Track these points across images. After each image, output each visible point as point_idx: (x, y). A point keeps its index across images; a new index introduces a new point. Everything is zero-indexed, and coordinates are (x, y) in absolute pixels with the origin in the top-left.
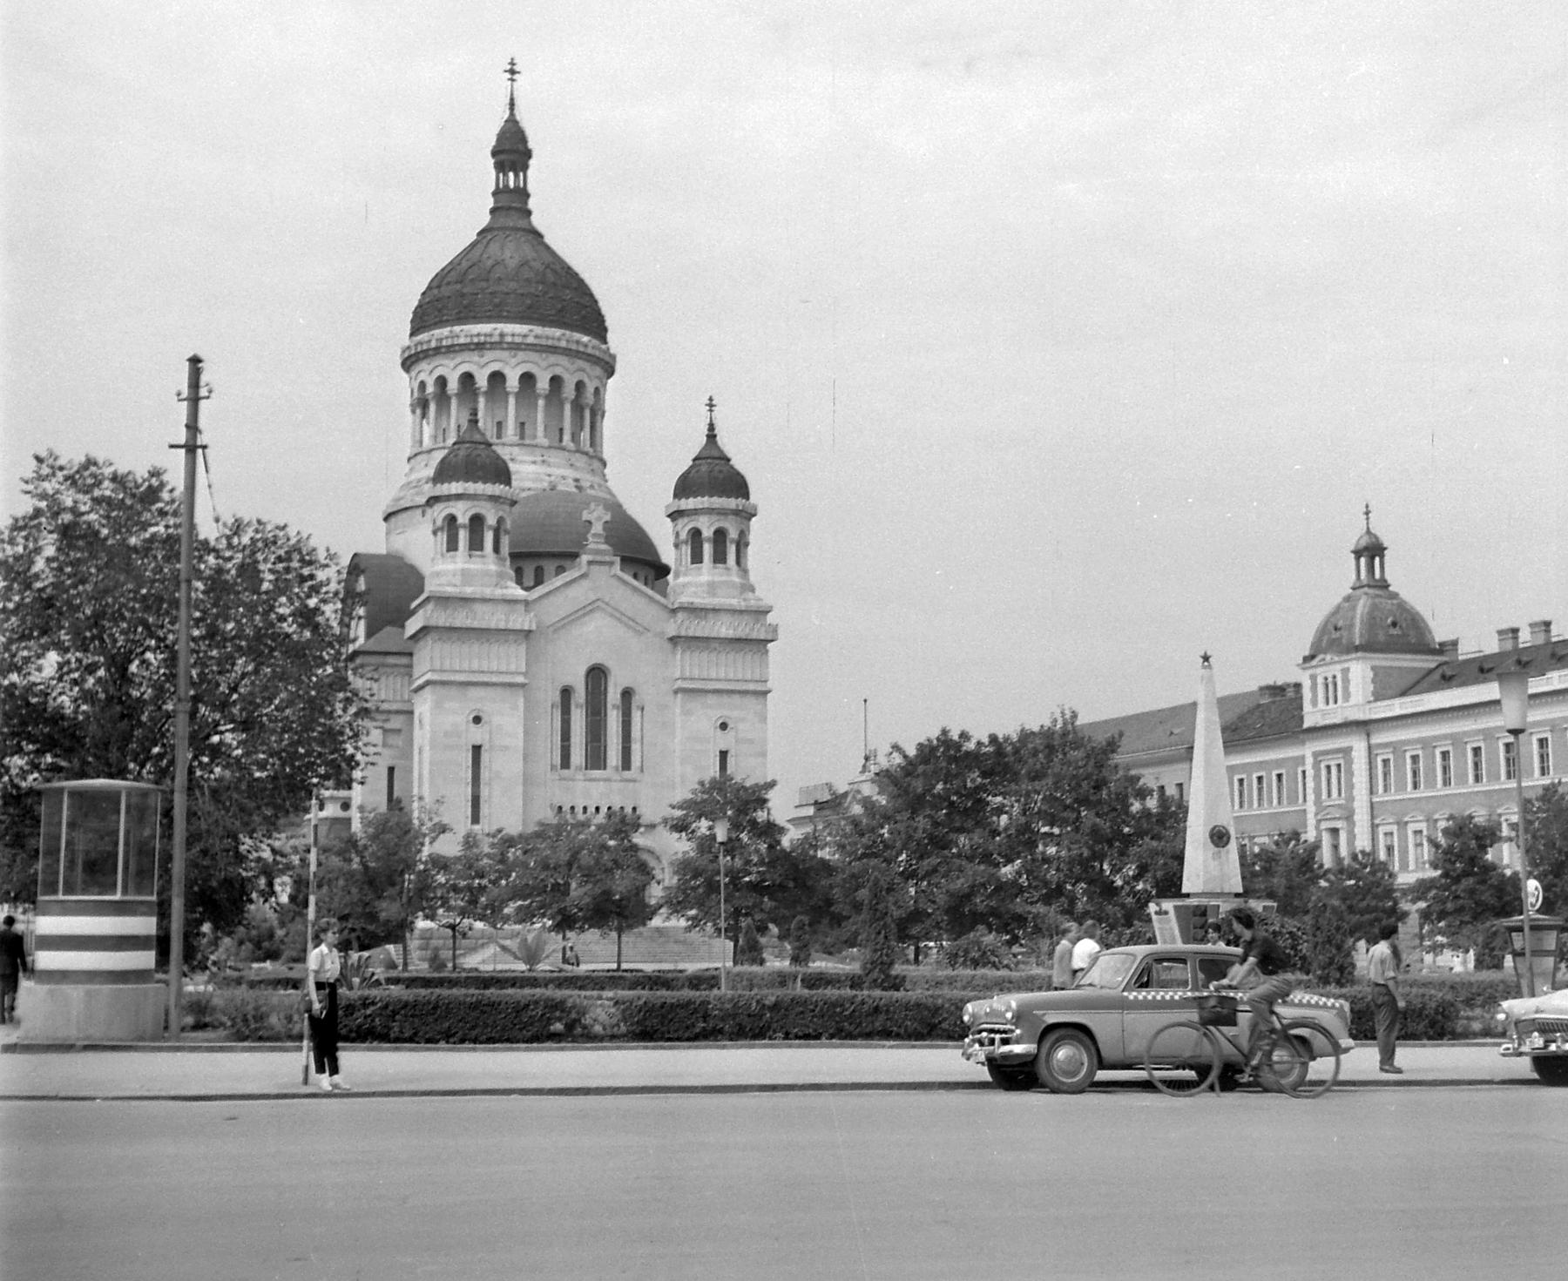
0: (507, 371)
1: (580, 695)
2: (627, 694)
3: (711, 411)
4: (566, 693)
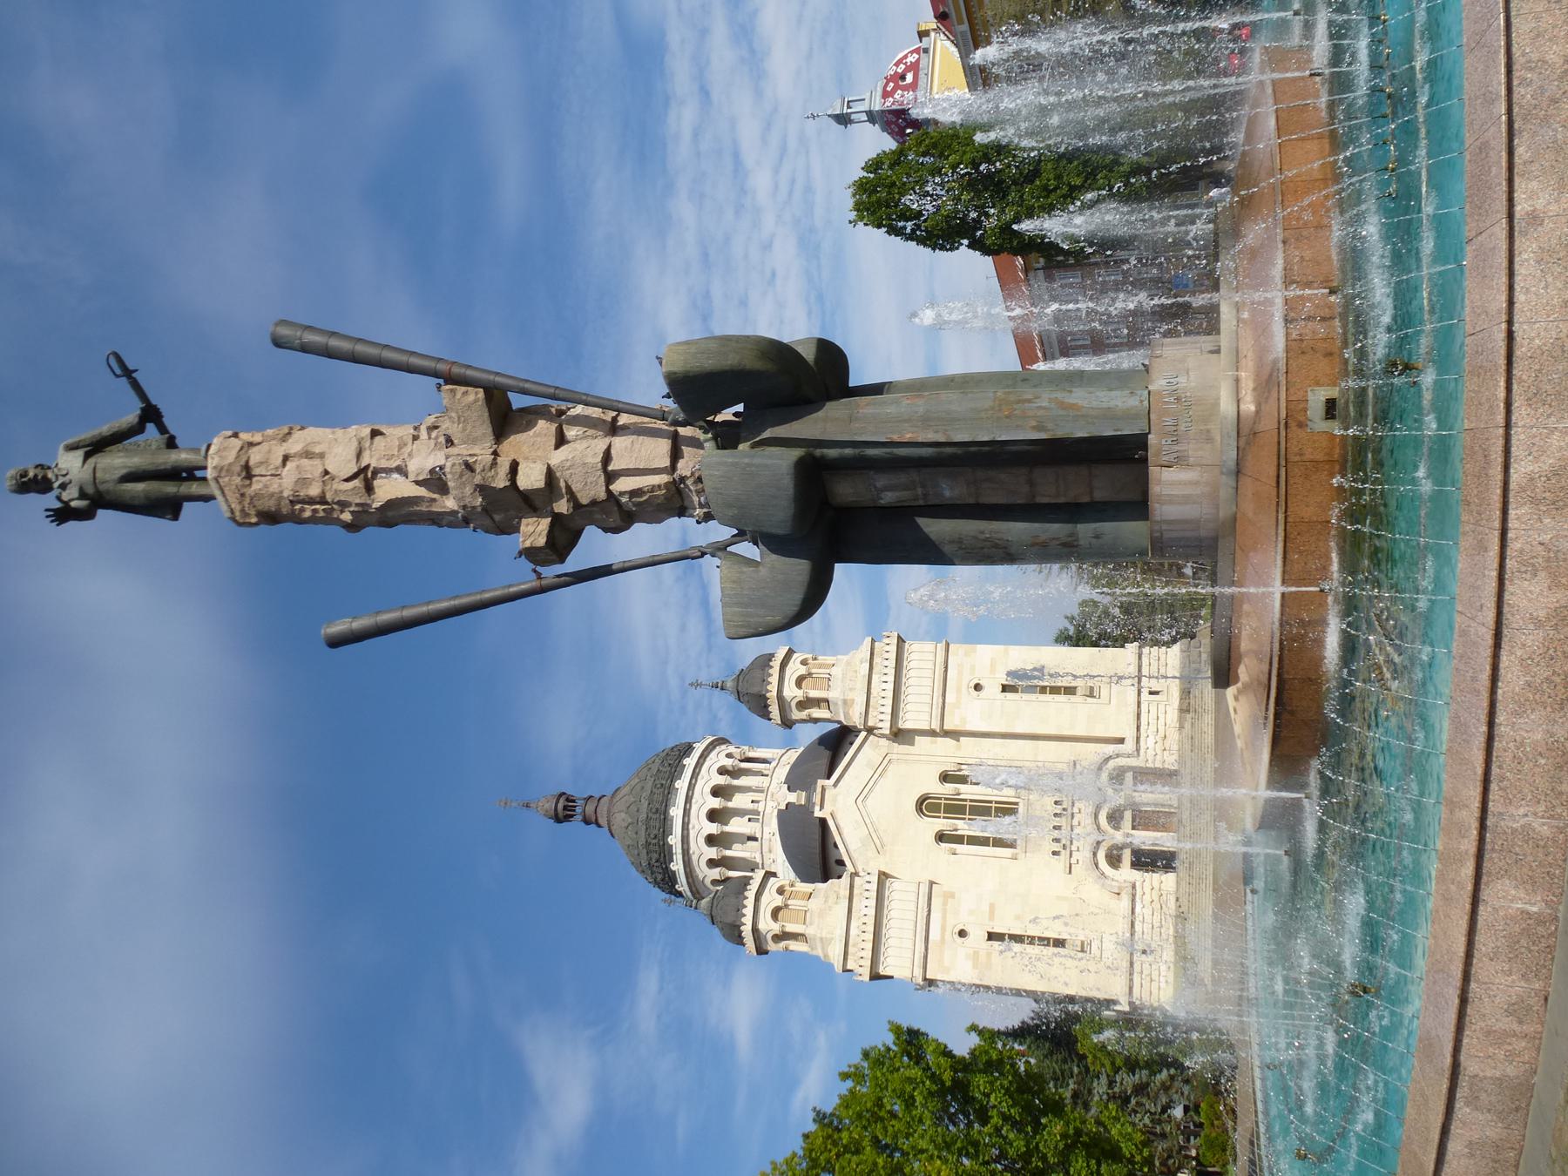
0: (705, 832)
1: (942, 824)
2: (945, 778)
3: (701, 685)
4: (941, 837)
